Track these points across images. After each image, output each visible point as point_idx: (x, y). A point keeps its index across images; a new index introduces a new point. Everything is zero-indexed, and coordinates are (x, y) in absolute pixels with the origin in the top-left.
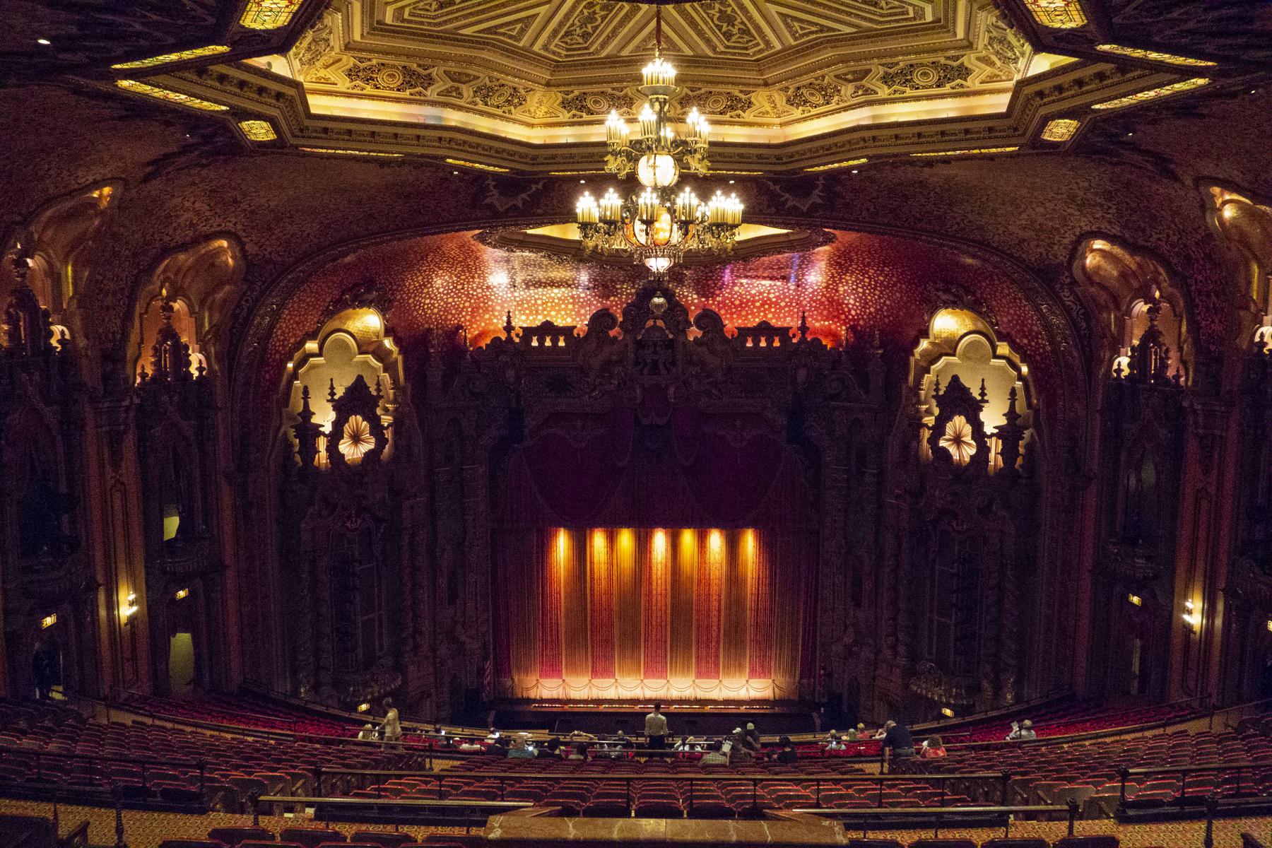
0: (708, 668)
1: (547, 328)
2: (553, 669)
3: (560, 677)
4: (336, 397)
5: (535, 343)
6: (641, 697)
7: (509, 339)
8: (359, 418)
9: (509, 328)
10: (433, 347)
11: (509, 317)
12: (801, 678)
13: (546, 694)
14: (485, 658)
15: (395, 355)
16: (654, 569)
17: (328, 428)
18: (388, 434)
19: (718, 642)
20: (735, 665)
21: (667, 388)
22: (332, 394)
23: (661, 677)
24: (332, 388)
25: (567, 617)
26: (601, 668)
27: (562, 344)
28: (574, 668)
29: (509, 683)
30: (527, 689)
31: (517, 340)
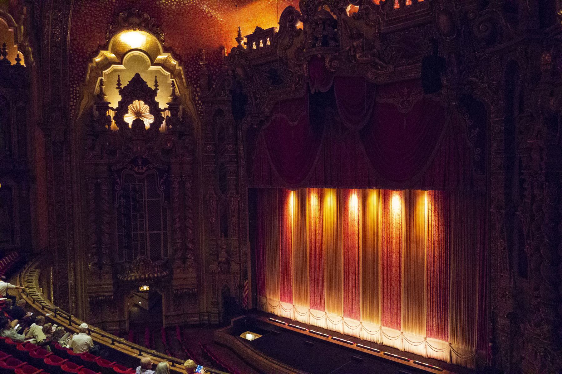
0: (392, 318)
1: (259, 34)
2: (287, 296)
3: (292, 303)
4: (122, 87)
5: (255, 47)
6: (342, 332)
7: (240, 46)
8: (142, 102)
9: (239, 39)
10: (202, 60)
11: (239, 32)
12: (479, 347)
13: (284, 314)
14: (246, 278)
15: (178, 67)
16: (350, 225)
17: (115, 105)
18: (164, 115)
19: (399, 295)
20: (414, 321)
21: (323, 59)
22: (119, 84)
23: (355, 318)
24: (119, 81)
25: (296, 257)
26: (317, 301)
27: (269, 43)
28: (300, 299)
29: (265, 300)
30: (274, 307)
31: (245, 47)
